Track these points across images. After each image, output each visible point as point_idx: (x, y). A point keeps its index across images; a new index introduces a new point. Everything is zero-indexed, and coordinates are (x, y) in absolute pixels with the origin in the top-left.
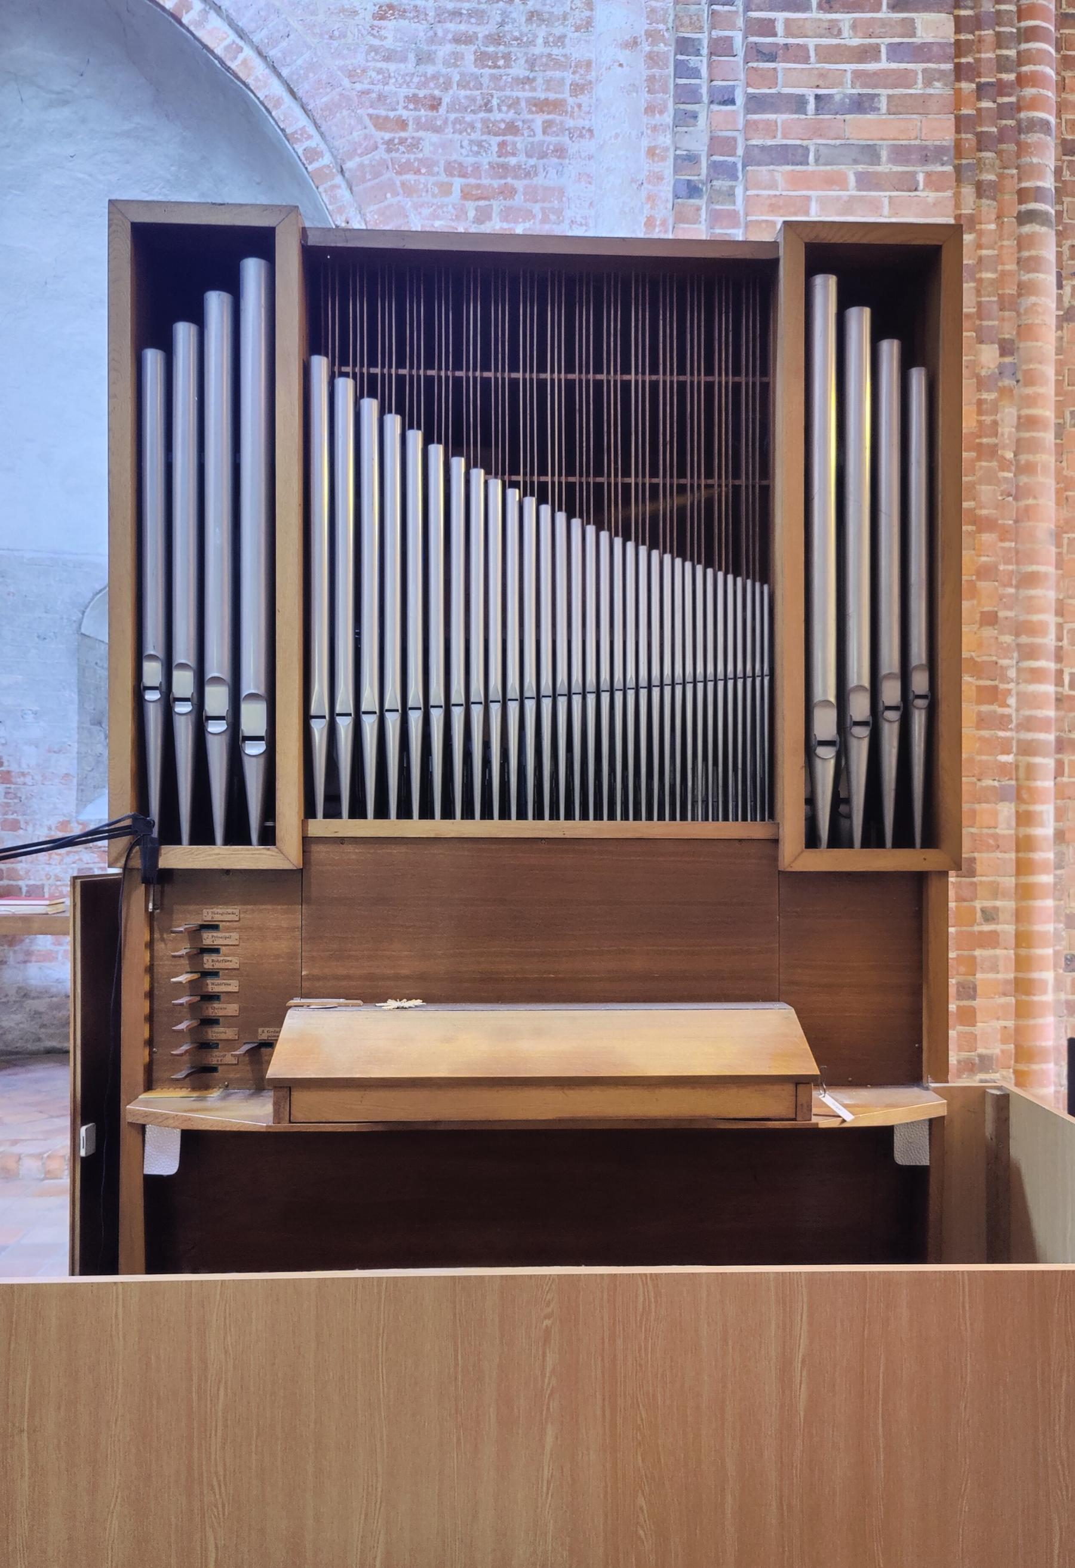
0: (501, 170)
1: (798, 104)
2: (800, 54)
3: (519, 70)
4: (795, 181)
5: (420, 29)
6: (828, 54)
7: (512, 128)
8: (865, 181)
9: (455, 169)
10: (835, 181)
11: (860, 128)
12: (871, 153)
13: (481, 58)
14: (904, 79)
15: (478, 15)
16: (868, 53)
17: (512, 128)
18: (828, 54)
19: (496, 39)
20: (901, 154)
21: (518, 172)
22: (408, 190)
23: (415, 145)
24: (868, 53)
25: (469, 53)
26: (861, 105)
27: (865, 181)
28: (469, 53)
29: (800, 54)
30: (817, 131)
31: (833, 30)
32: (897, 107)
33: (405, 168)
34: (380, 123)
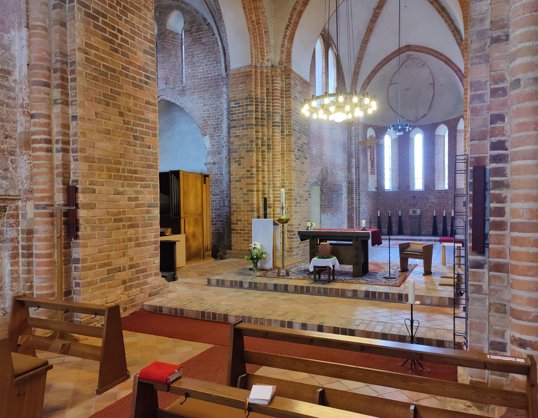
0: (217, 124)
1: (235, 120)
2: (235, 114)
3: (219, 111)
4: (235, 130)
5: (208, 107)
6: (239, 113)
7: (218, 119)
8: (243, 129)
9: (212, 125)
10: (240, 130)
11: (243, 122)
12: (243, 125)
13: (215, 110)
14: (247, 115)
15: (214, 104)
16: (243, 112)
17: (218, 119)
18: (239, 113)
19: (216, 107)
20: (247, 125)
21: (219, 124)
22: (207, 129)
23: (207, 123)
24: (243, 112)
25: (213, 109)
26: (243, 119)
27: (243, 129)
28: (213, 109)
29: (235, 114)
30: (237, 123)
31: (239, 110)
32: (246, 119)
33: (207, 126)
34: (204, 120)
